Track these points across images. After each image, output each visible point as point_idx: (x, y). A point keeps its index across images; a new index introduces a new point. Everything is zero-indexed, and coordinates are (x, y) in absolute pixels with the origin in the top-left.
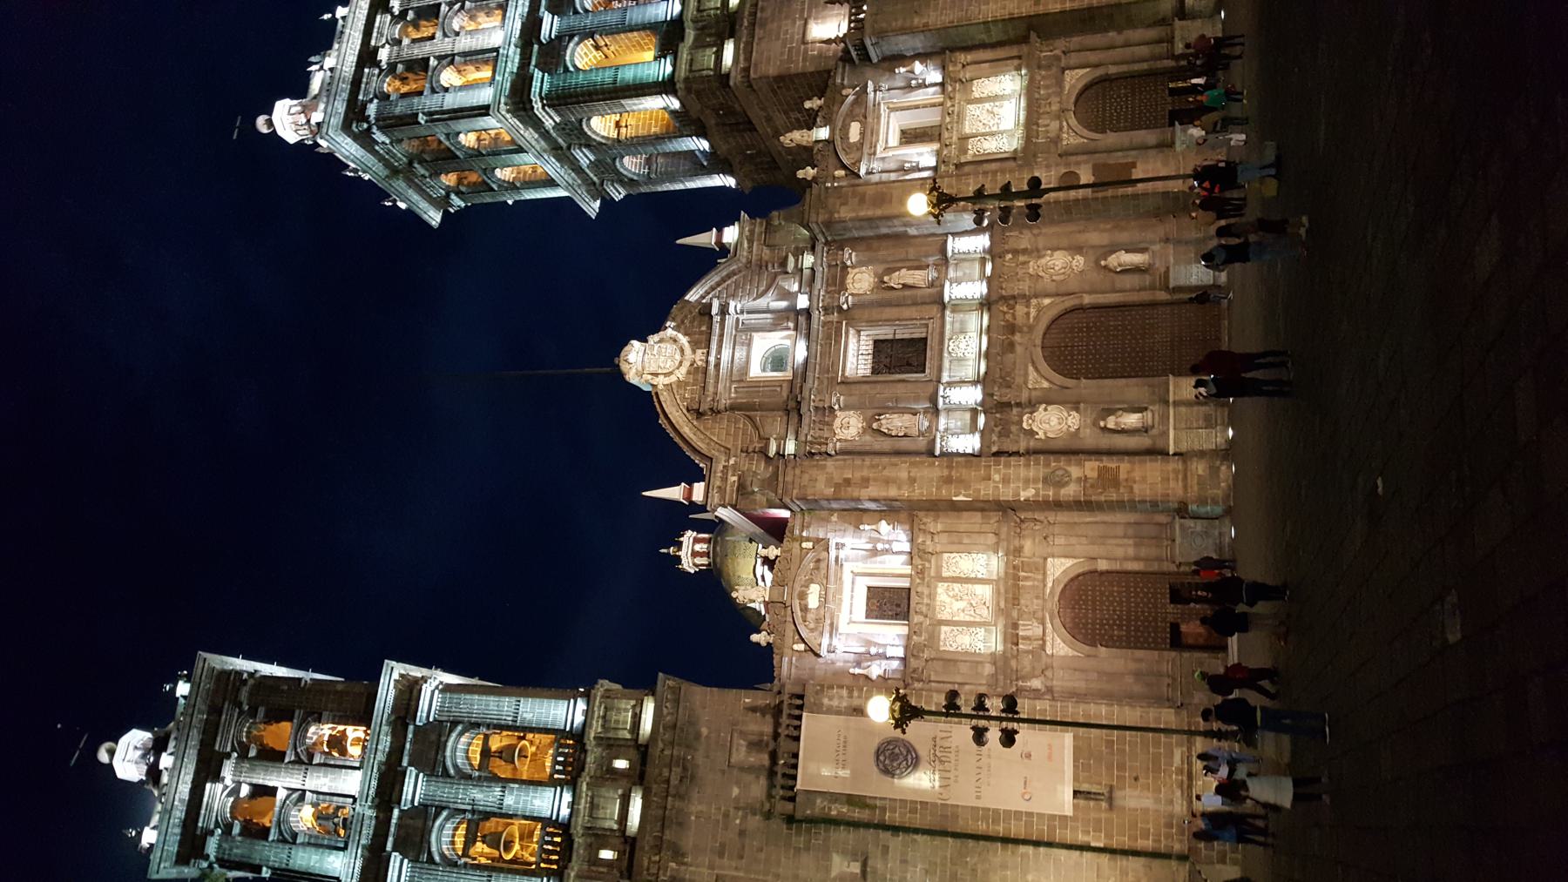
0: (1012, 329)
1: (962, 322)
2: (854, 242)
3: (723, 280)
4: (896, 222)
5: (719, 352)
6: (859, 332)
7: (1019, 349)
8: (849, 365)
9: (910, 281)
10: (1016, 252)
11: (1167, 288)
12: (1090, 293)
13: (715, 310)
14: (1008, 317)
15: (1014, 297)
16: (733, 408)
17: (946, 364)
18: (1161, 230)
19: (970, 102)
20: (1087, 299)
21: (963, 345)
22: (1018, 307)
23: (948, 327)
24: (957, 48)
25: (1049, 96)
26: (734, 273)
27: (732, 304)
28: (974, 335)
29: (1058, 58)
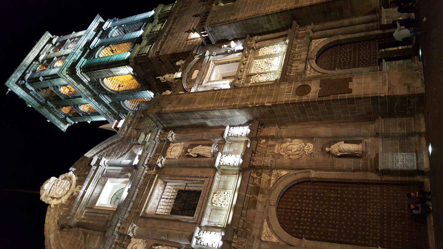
0: (257, 190)
1: (226, 182)
2: (176, 129)
3: (108, 147)
4: (197, 115)
5: (87, 188)
6: (165, 183)
7: (259, 207)
8: (151, 205)
9: (201, 153)
10: (267, 138)
11: (376, 171)
12: (316, 169)
13: (93, 163)
14: (256, 181)
15: (261, 167)
16: (79, 225)
17: (208, 211)
18: (372, 127)
19: (256, 58)
20: (313, 174)
21: (221, 199)
22: (264, 175)
23: (215, 184)
24: (255, 33)
25: (301, 51)
26: (114, 143)
27: (104, 160)
28: (231, 192)
29: (309, 33)
